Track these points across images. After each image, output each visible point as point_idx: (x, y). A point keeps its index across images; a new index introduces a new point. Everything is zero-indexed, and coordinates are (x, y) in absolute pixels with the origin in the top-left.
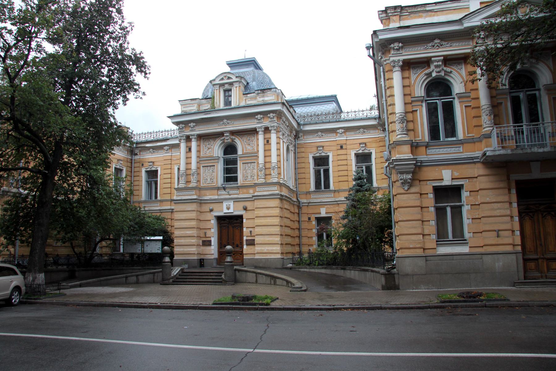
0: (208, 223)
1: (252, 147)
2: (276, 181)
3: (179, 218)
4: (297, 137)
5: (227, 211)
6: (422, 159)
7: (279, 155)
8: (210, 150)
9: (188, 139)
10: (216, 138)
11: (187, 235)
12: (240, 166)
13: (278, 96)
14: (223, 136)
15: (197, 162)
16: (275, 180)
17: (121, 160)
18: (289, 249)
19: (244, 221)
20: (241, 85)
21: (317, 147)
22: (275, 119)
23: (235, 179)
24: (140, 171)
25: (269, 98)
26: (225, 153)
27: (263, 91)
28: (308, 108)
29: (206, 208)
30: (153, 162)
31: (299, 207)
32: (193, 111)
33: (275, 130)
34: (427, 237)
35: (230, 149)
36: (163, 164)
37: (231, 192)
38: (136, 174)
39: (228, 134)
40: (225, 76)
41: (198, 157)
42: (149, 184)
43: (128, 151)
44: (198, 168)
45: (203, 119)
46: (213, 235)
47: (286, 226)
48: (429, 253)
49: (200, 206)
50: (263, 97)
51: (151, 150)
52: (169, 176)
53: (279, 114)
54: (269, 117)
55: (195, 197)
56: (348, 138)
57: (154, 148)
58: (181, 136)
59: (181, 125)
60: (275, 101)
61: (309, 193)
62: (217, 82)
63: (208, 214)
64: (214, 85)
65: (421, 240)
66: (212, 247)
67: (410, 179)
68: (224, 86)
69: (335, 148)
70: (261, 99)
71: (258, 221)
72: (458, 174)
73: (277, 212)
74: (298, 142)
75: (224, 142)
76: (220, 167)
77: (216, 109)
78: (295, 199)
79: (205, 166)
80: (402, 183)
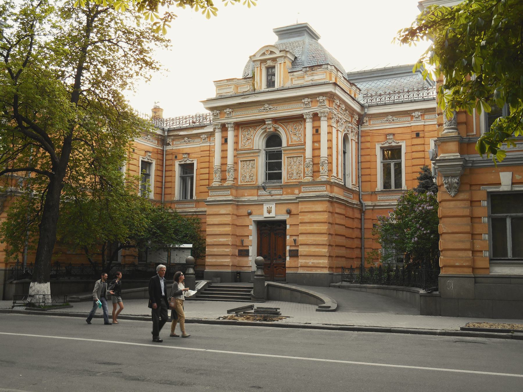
0: (246, 229)
1: (299, 137)
2: (325, 179)
3: (212, 223)
4: (360, 122)
6: (475, 159)
7: (330, 148)
8: (250, 141)
9: (224, 128)
10: (257, 126)
11: (221, 243)
12: (285, 161)
13: (330, 74)
14: (265, 124)
16: (324, 178)
17: (149, 152)
18: (343, 263)
19: (288, 227)
20: (287, 60)
21: (386, 135)
22: (326, 103)
23: (279, 176)
24: (173, 165)
25: (319, 76)
27: (312, 68)
28: (384, 81)
29: (244, 211)
30: (189, 154)
31: (362, 211)
32: (229, 94)
33: (325, 116)
34: (478, 254)
35: (273, 140)
36: (199, 156)
37: (273, 192)
38: (168, 168)
39: (269, 122)
40: (267, 51)
41: (236, 150)
42: (183, 179)
43: (158, 140)
44: (236, 163)
45: (240, 104)
46: (252, 243)
47: (336, 235)
48: (480, 273)
49: (237, 209)
50: (312, 76)
51: (186, 139)
52: (206, 171)
53: (331, 97)
54: (318, 101)
55: (230, 198)
56: (426, 124)
57: (189, 136)
58: (216, 125)
59: (215, 112)
60: (327, 80)
61: (374, 193)
62: (258, 58)
63: (246, 218)
64: (254, 61)
65: (470, 257)
66: (250, 258)
67: (457, 183)
68: (267, 62)
69: (408, 136)
70: (311, 78)
71: (302, 228)
72: (521, 177)
73: (324, 217)
74: (363, 129)
75: (265, 131)
76: (261, 161)
77: (256, 92)
78: (355, 202)
79: (244, 161)
80: (447, 188)
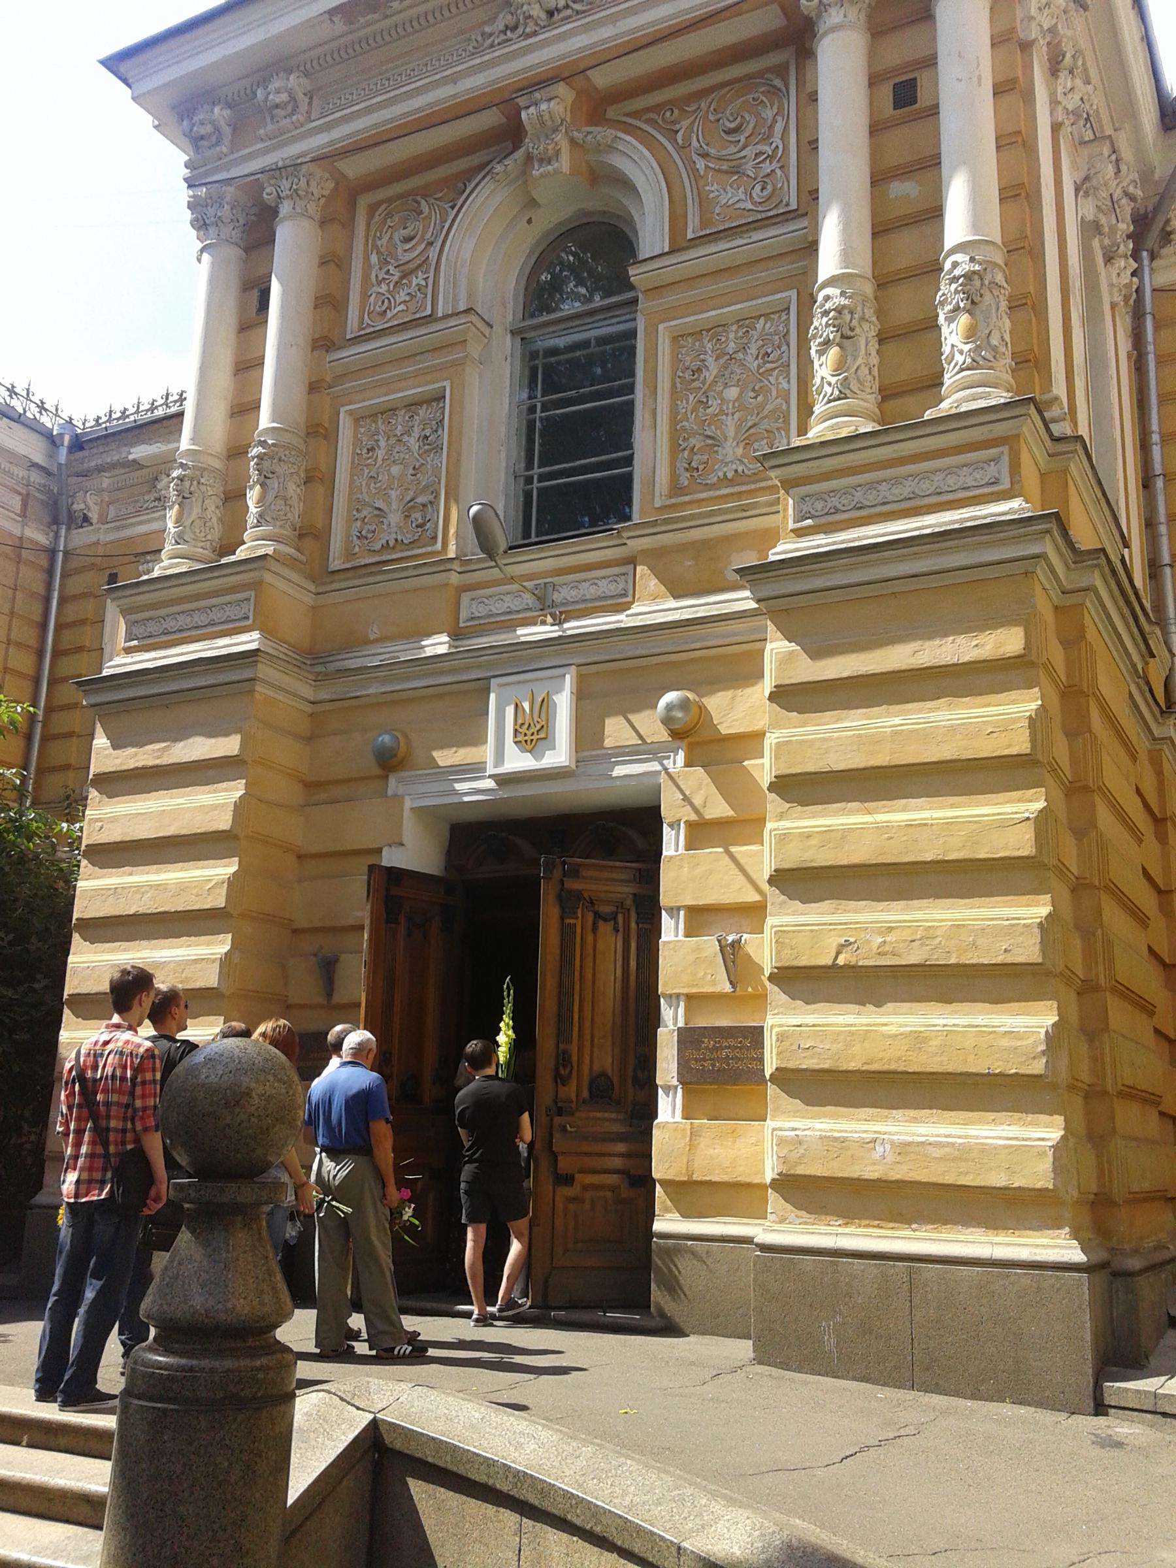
5: (518, 761)
8: (417, 280)
15: (314, 387)
19: (672, 843)
26: (540, 296)
41: (324, 343)
44: (317, 432)
